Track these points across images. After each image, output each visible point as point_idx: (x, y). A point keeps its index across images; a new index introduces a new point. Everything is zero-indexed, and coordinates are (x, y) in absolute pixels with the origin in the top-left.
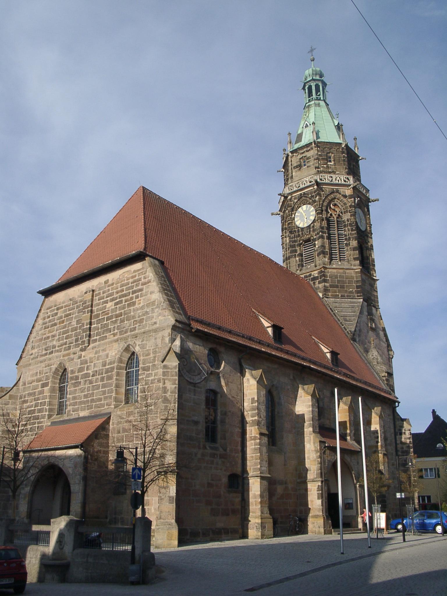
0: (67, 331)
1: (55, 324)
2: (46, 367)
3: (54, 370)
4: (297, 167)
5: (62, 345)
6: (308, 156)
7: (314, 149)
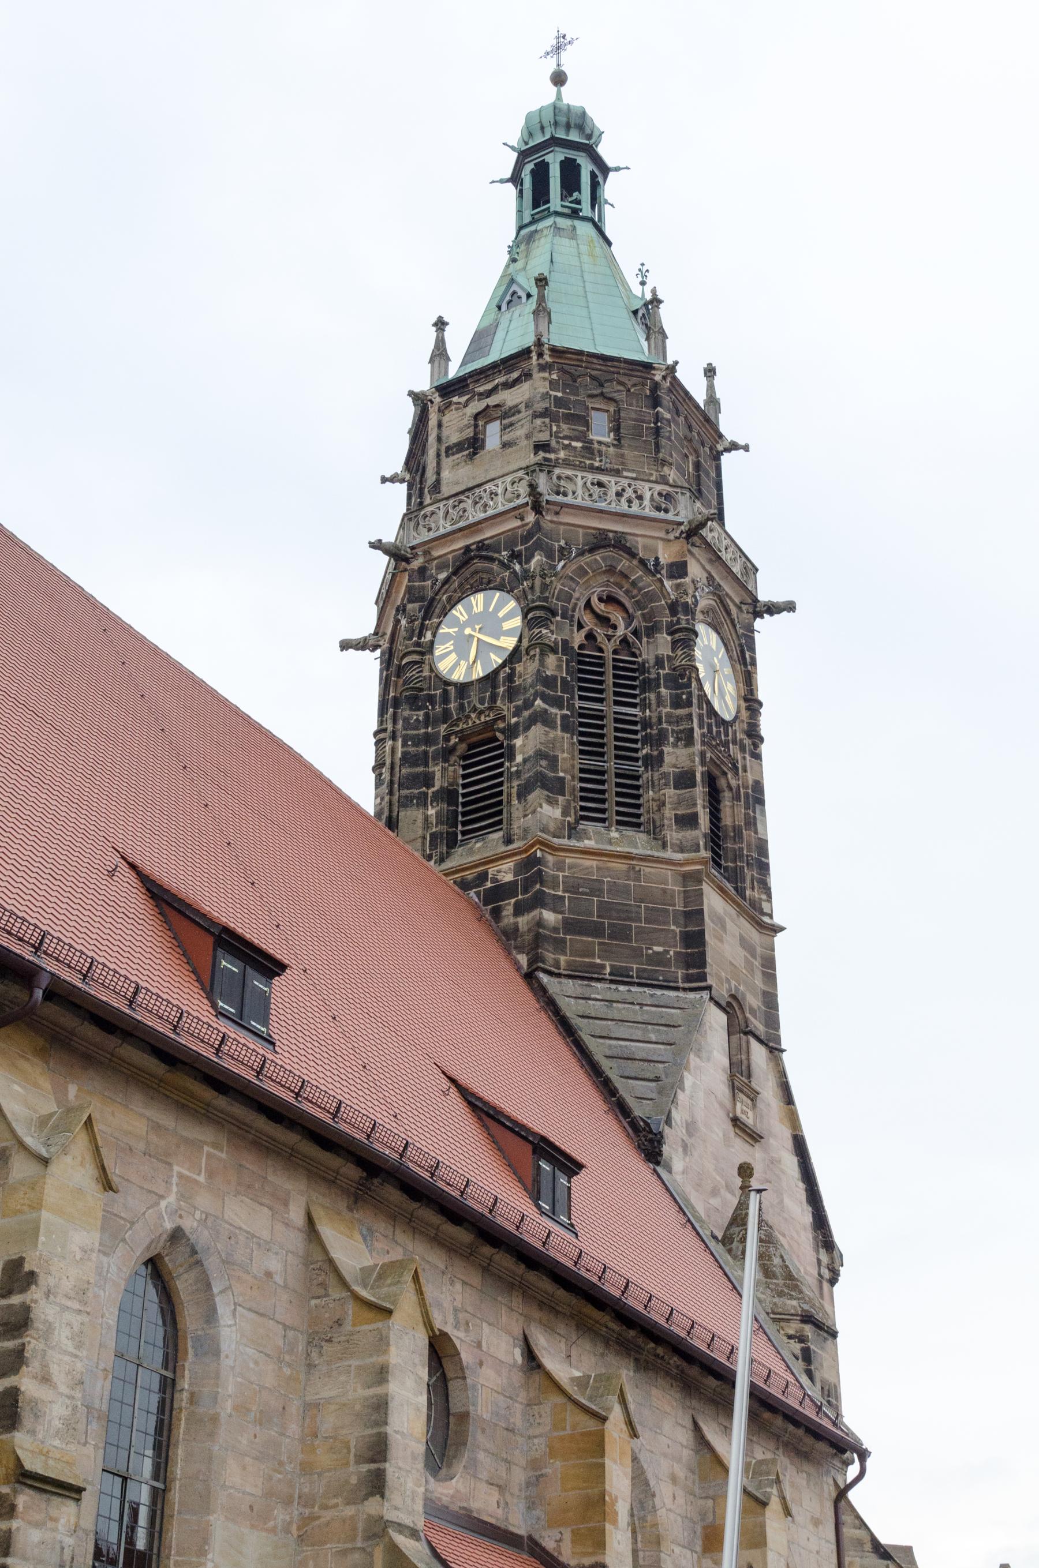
4: (459, 447)
6: (510, 403)
7: (537, 375)
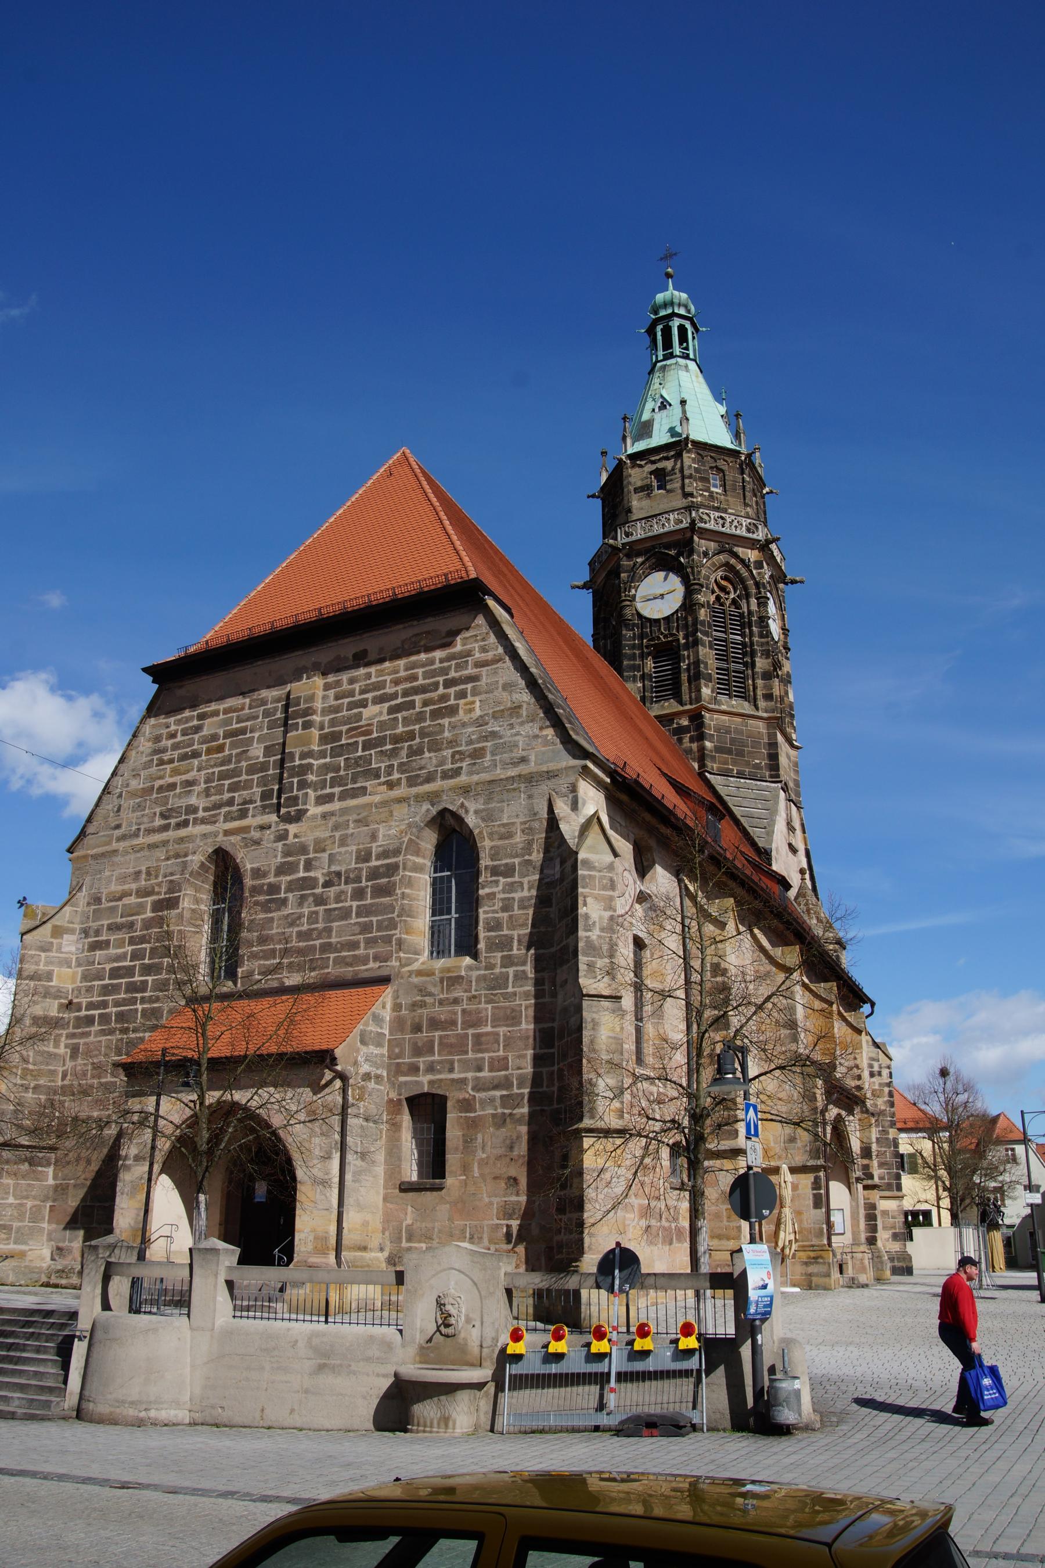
0: (236, 772)
1: (196, 755)
2: (168, 859)
3: (196, 867)
5: (217, 806)
